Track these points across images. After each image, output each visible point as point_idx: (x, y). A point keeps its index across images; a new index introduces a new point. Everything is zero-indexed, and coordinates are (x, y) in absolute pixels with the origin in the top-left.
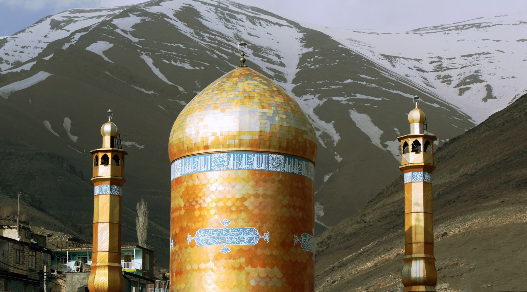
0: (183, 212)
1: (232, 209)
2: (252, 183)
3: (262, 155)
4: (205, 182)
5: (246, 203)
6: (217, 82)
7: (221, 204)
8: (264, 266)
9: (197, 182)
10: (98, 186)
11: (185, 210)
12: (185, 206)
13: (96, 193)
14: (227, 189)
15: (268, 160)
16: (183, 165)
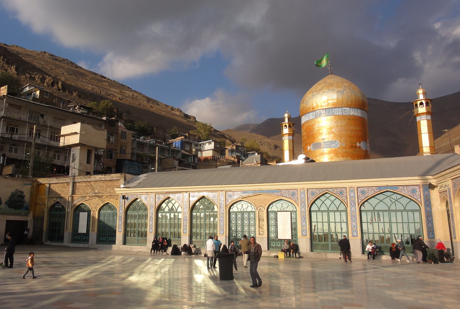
2: (335, 121)
8: (343, 157)
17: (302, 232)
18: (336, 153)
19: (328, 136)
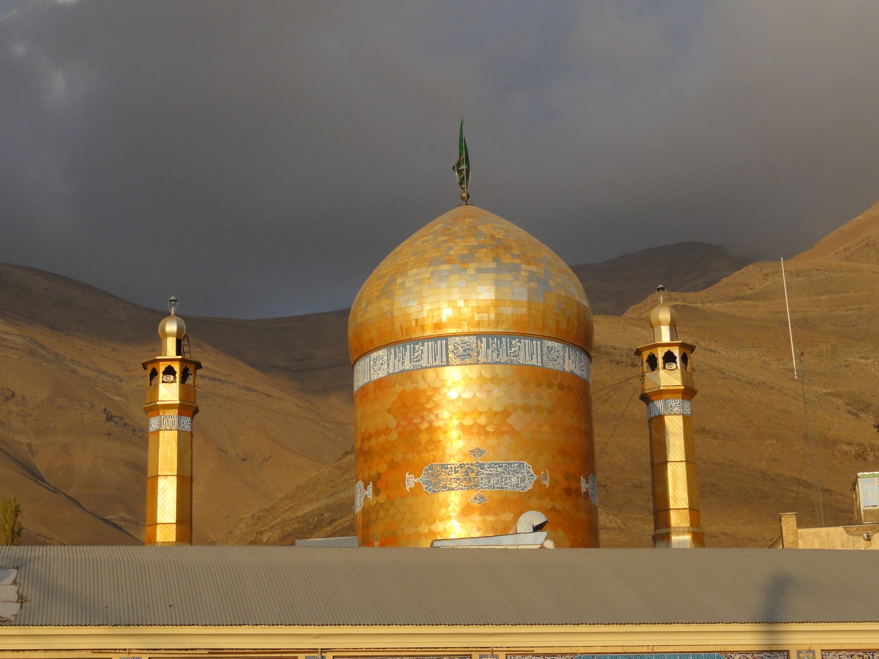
0: (393, 436)
1: (488, 429)
3: (532, 341)
4: (438, 384)
5: (511, 420)
6: (437, 225)
7: (468, 422)
9: (422, 385)
10: (157, 418)
11: (399, 433)
12: (398, 425)
13: (151, 429)
14: (478, 395)
15: (542, 351)
16: (392, 357)
19: (492, 441)
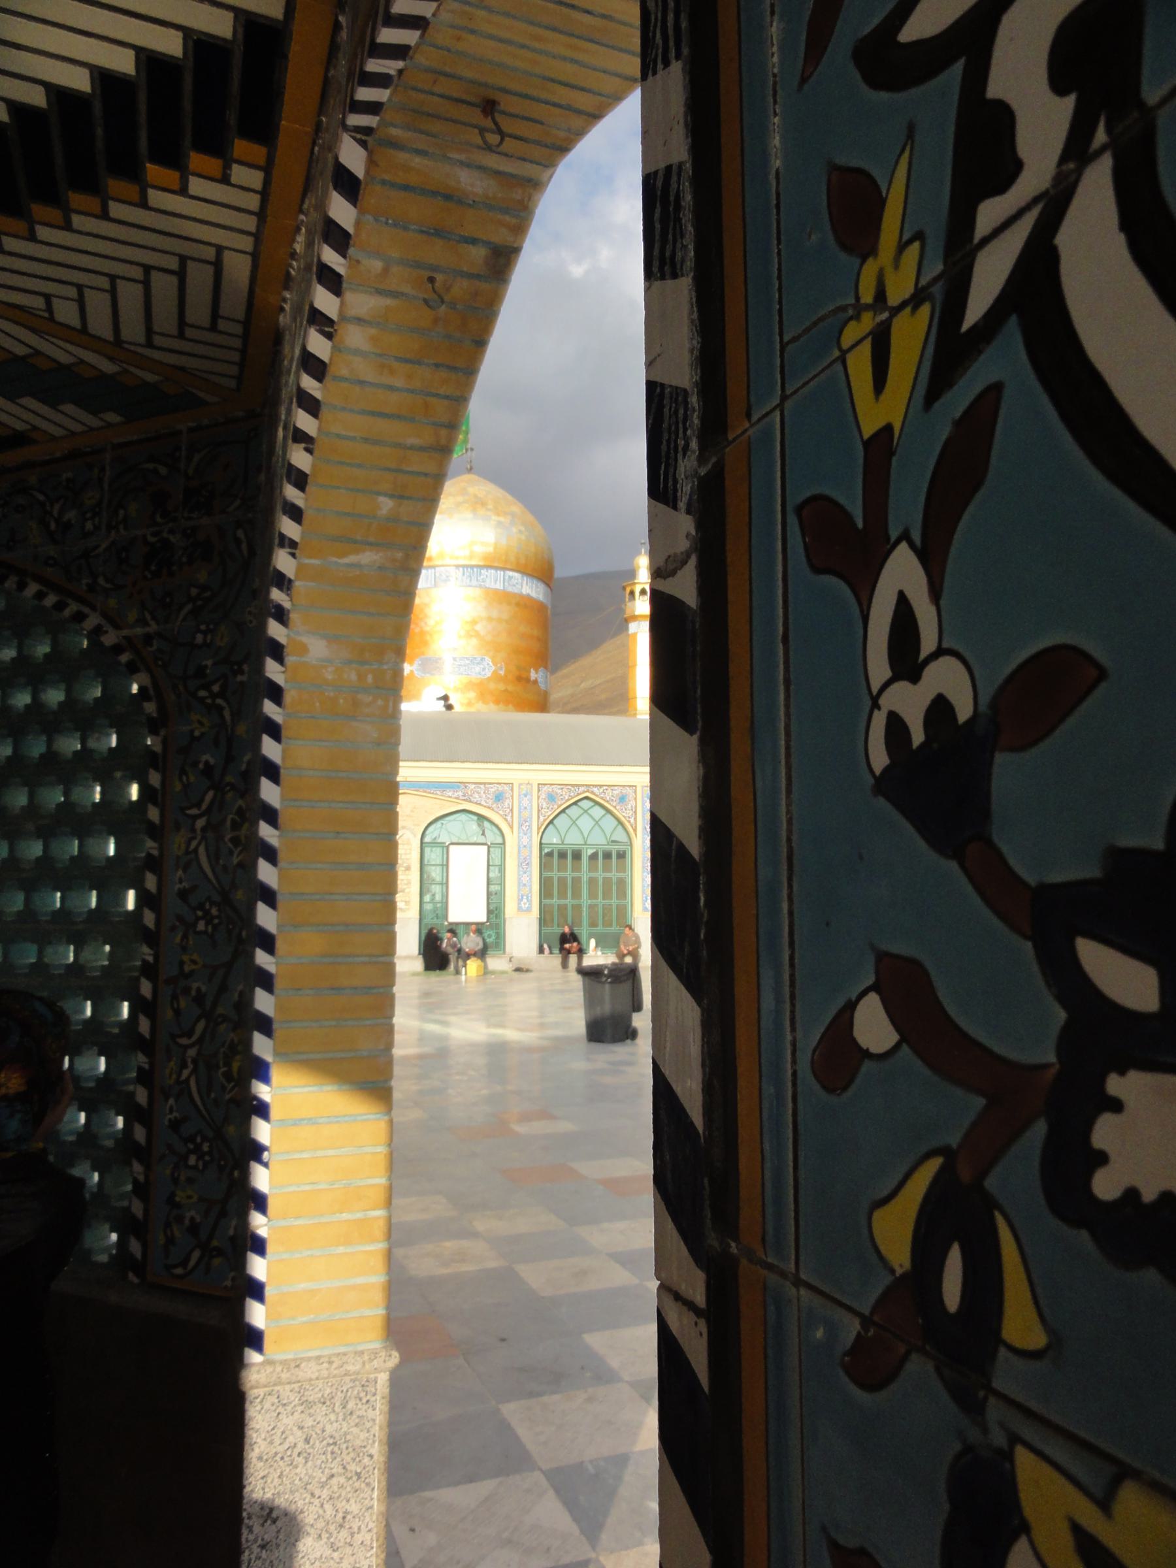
5: (478, 627)
8: (497, 702)
17: (520, 900)
18: (482, 690)
